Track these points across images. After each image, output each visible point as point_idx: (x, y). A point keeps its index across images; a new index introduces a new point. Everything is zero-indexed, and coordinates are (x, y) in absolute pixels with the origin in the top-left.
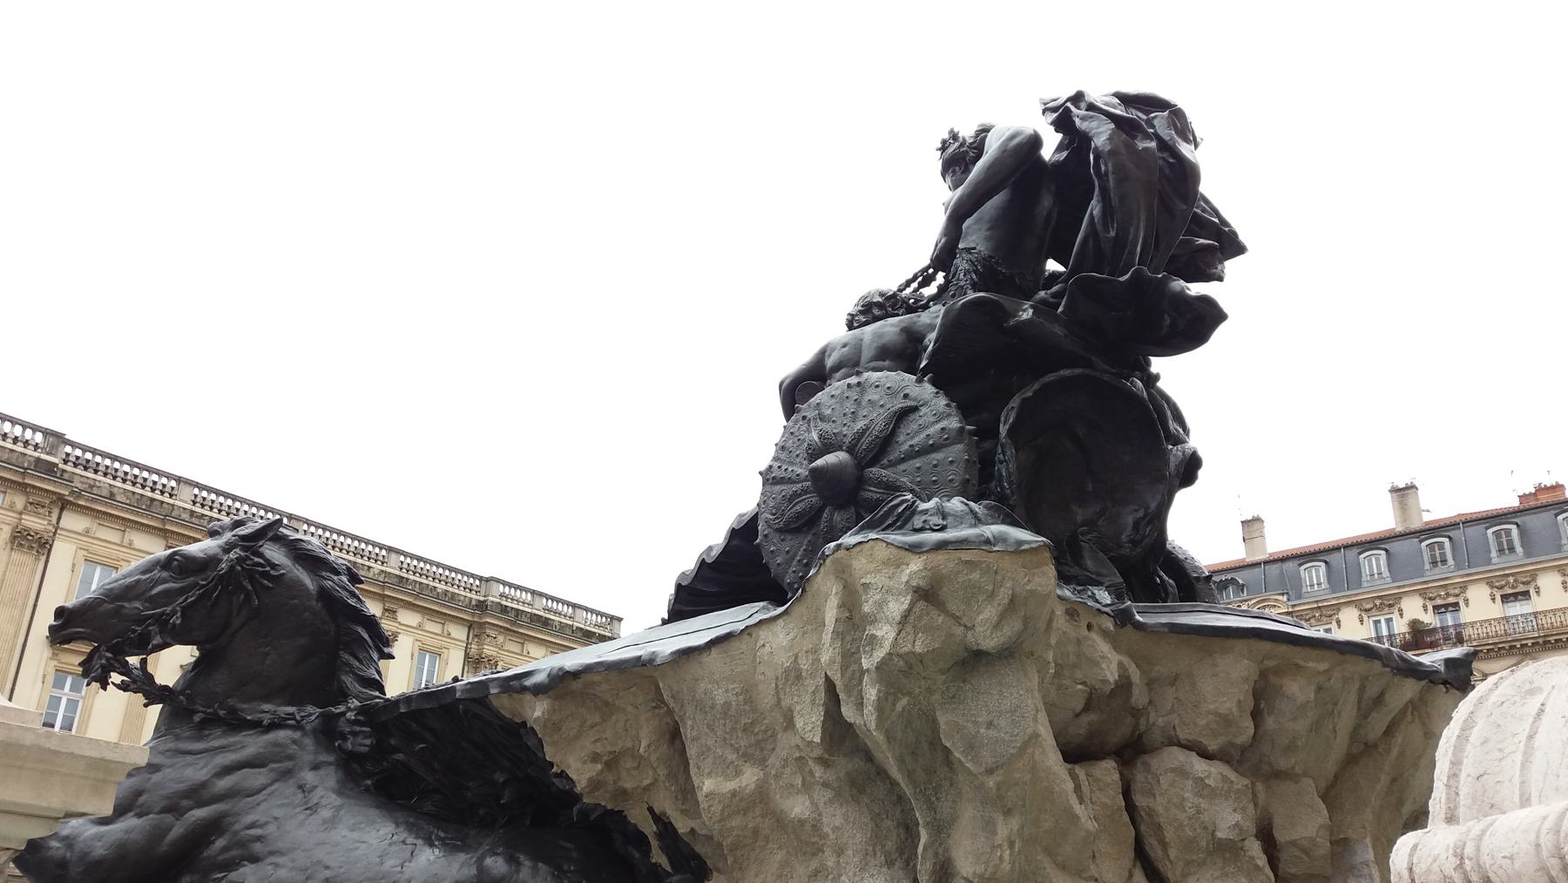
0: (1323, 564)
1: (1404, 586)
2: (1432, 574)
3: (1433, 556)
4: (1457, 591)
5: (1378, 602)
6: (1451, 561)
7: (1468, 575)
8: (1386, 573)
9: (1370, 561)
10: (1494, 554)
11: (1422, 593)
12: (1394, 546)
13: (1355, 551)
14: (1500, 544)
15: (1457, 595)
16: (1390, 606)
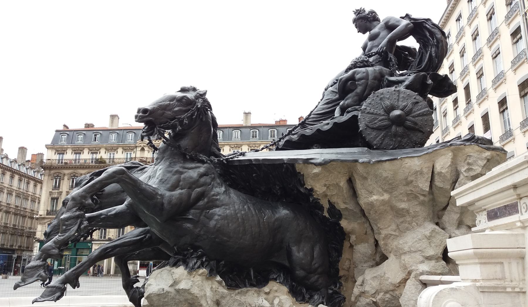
0: (222, 132)
1: (244, 142)
2: (252, 140)
3: (253, 135)
4: (258, 146)
5: (236, 146)
6: (258, 137)
7: (262, 142)
8: (239, 137)
9: (235, 133)
10: (269, 137)
11: (248, 145)
12: (242, 130)
13: (232, 129)
14: (271, 134)
15: (258, 147)
16: (239, 147)
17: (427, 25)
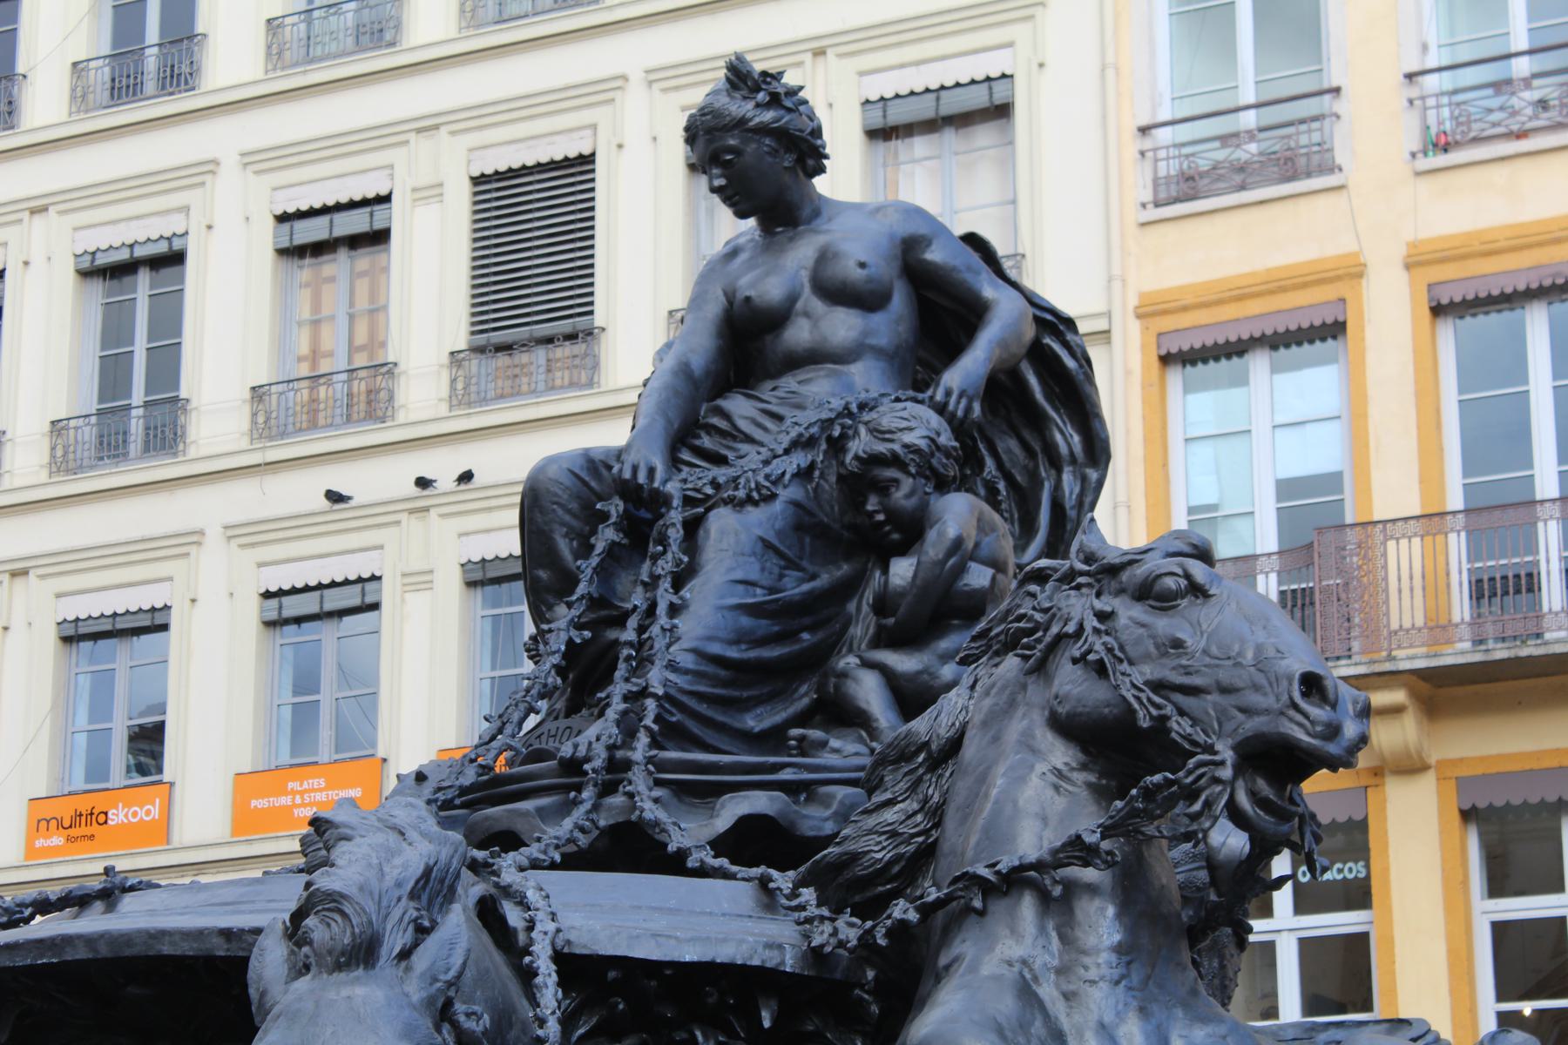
17: (1057, 347)
